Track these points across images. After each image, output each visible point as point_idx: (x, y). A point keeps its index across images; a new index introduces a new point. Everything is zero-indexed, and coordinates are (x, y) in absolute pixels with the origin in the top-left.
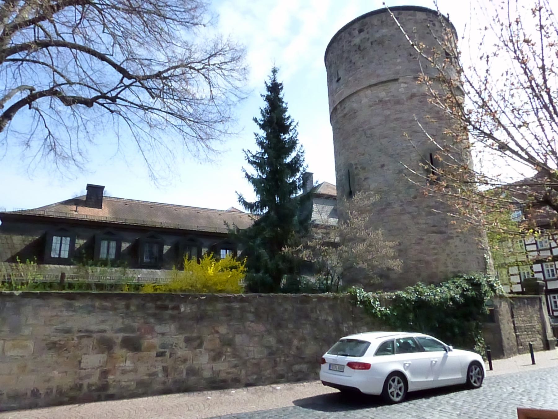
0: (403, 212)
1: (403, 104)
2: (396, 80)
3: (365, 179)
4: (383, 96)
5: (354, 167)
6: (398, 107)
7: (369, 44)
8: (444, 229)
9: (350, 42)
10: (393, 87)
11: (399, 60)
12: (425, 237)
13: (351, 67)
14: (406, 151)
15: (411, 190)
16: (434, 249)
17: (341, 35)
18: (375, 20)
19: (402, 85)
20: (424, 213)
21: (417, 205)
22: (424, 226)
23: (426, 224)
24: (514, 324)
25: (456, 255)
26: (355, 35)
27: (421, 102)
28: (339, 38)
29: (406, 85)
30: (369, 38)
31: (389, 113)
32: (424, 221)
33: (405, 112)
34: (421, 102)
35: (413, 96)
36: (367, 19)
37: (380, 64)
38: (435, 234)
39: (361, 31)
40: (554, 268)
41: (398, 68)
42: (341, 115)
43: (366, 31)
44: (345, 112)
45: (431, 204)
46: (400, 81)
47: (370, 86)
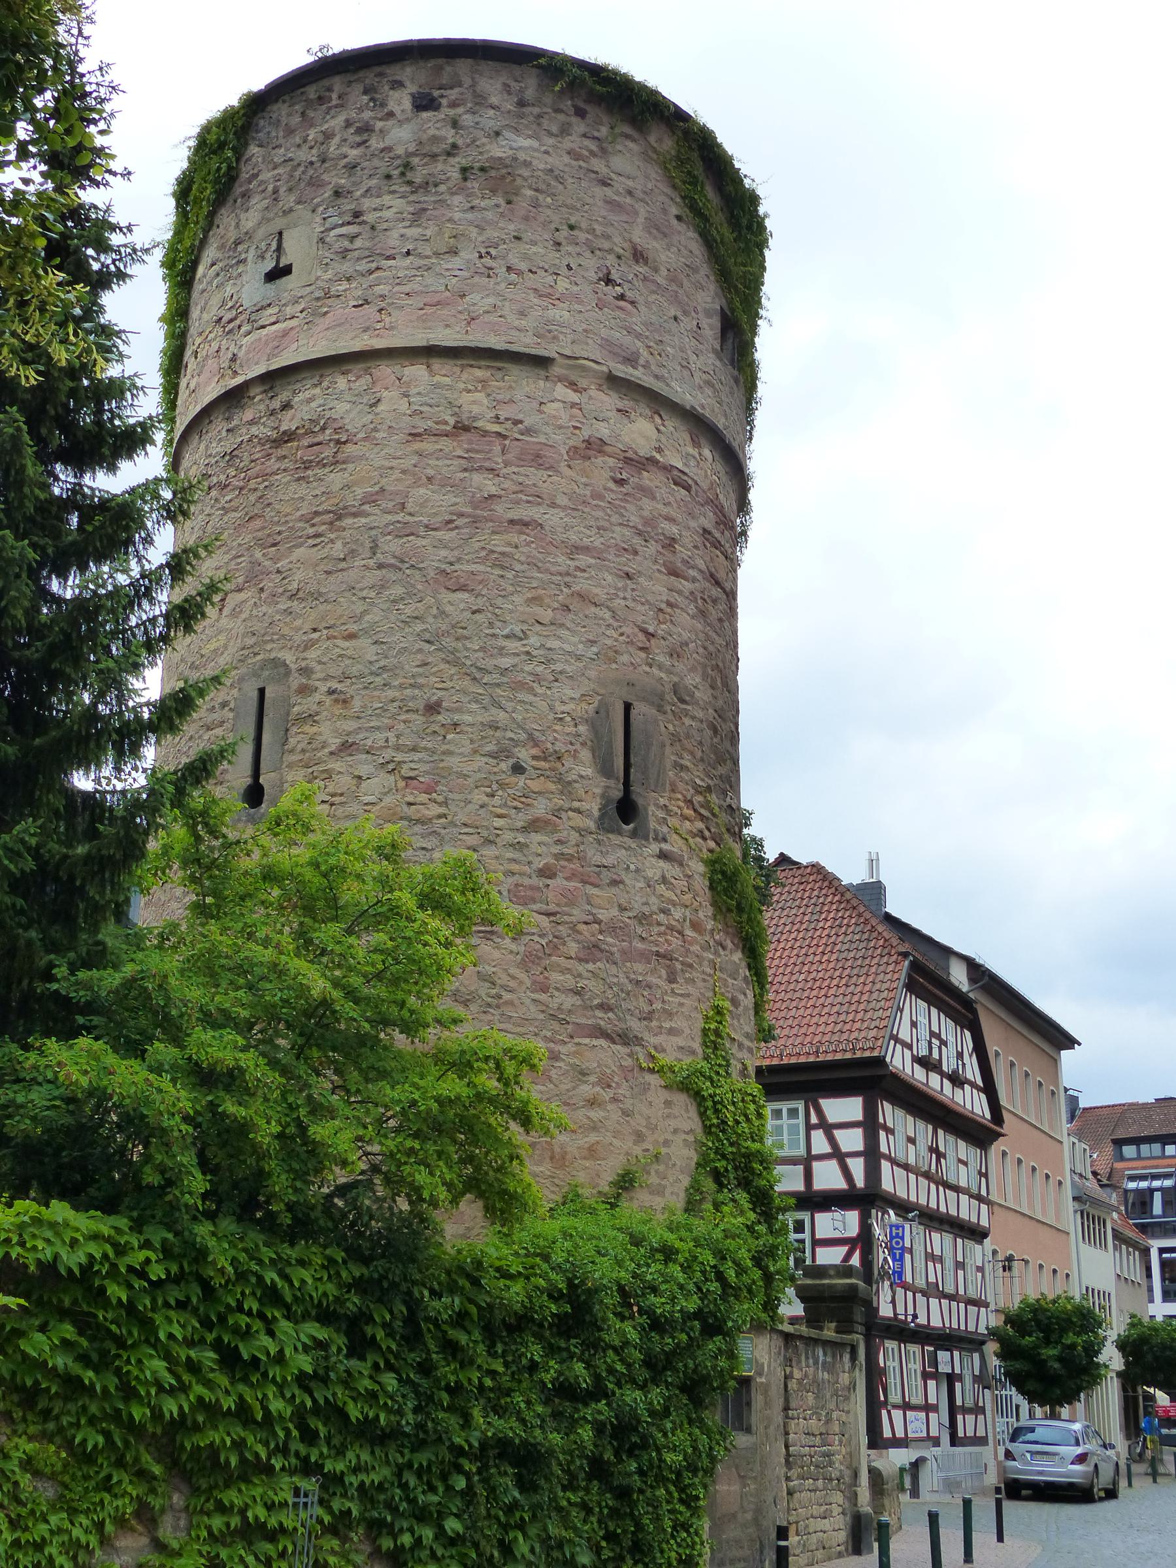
2: (541, 362)
3: (347, 747)
4: (476, 409)
5: (296, 681)
6: (534, 476)
7: (456, 175)
8: (635, 1025)
9: (366, 129)
10: (523, 385)
12: (563, 1049)
13: (352, 238)
14: (540, 669)
15: (536, 838)
16: (592, 1103)
17: (326, 82)
18: (493, 84)
19: (561, 391)
20: (573, 948)
21: (552, 908)
22: (569, 1001)
23: (578, 992)
24: (787, 1447)
25: (666, 1143)
26: (392, 106)
27: (621, 482)
28: (312, 92)
29: (573, 397)
30: (454, 146)
31: (494, 490)
32: (569, 981)
33: (553, 505)
34: (621, 482)
35: (594, 447)
36: (462, 67)
37: (489, 272)
38: (602, 1042)
39: (424, 103)
40: (806, 1236)
41: (553, 313)
43: (446, 112)
44: (288, 422)
45: (603, 915)
46: (556, 370)
47: (429, 352)
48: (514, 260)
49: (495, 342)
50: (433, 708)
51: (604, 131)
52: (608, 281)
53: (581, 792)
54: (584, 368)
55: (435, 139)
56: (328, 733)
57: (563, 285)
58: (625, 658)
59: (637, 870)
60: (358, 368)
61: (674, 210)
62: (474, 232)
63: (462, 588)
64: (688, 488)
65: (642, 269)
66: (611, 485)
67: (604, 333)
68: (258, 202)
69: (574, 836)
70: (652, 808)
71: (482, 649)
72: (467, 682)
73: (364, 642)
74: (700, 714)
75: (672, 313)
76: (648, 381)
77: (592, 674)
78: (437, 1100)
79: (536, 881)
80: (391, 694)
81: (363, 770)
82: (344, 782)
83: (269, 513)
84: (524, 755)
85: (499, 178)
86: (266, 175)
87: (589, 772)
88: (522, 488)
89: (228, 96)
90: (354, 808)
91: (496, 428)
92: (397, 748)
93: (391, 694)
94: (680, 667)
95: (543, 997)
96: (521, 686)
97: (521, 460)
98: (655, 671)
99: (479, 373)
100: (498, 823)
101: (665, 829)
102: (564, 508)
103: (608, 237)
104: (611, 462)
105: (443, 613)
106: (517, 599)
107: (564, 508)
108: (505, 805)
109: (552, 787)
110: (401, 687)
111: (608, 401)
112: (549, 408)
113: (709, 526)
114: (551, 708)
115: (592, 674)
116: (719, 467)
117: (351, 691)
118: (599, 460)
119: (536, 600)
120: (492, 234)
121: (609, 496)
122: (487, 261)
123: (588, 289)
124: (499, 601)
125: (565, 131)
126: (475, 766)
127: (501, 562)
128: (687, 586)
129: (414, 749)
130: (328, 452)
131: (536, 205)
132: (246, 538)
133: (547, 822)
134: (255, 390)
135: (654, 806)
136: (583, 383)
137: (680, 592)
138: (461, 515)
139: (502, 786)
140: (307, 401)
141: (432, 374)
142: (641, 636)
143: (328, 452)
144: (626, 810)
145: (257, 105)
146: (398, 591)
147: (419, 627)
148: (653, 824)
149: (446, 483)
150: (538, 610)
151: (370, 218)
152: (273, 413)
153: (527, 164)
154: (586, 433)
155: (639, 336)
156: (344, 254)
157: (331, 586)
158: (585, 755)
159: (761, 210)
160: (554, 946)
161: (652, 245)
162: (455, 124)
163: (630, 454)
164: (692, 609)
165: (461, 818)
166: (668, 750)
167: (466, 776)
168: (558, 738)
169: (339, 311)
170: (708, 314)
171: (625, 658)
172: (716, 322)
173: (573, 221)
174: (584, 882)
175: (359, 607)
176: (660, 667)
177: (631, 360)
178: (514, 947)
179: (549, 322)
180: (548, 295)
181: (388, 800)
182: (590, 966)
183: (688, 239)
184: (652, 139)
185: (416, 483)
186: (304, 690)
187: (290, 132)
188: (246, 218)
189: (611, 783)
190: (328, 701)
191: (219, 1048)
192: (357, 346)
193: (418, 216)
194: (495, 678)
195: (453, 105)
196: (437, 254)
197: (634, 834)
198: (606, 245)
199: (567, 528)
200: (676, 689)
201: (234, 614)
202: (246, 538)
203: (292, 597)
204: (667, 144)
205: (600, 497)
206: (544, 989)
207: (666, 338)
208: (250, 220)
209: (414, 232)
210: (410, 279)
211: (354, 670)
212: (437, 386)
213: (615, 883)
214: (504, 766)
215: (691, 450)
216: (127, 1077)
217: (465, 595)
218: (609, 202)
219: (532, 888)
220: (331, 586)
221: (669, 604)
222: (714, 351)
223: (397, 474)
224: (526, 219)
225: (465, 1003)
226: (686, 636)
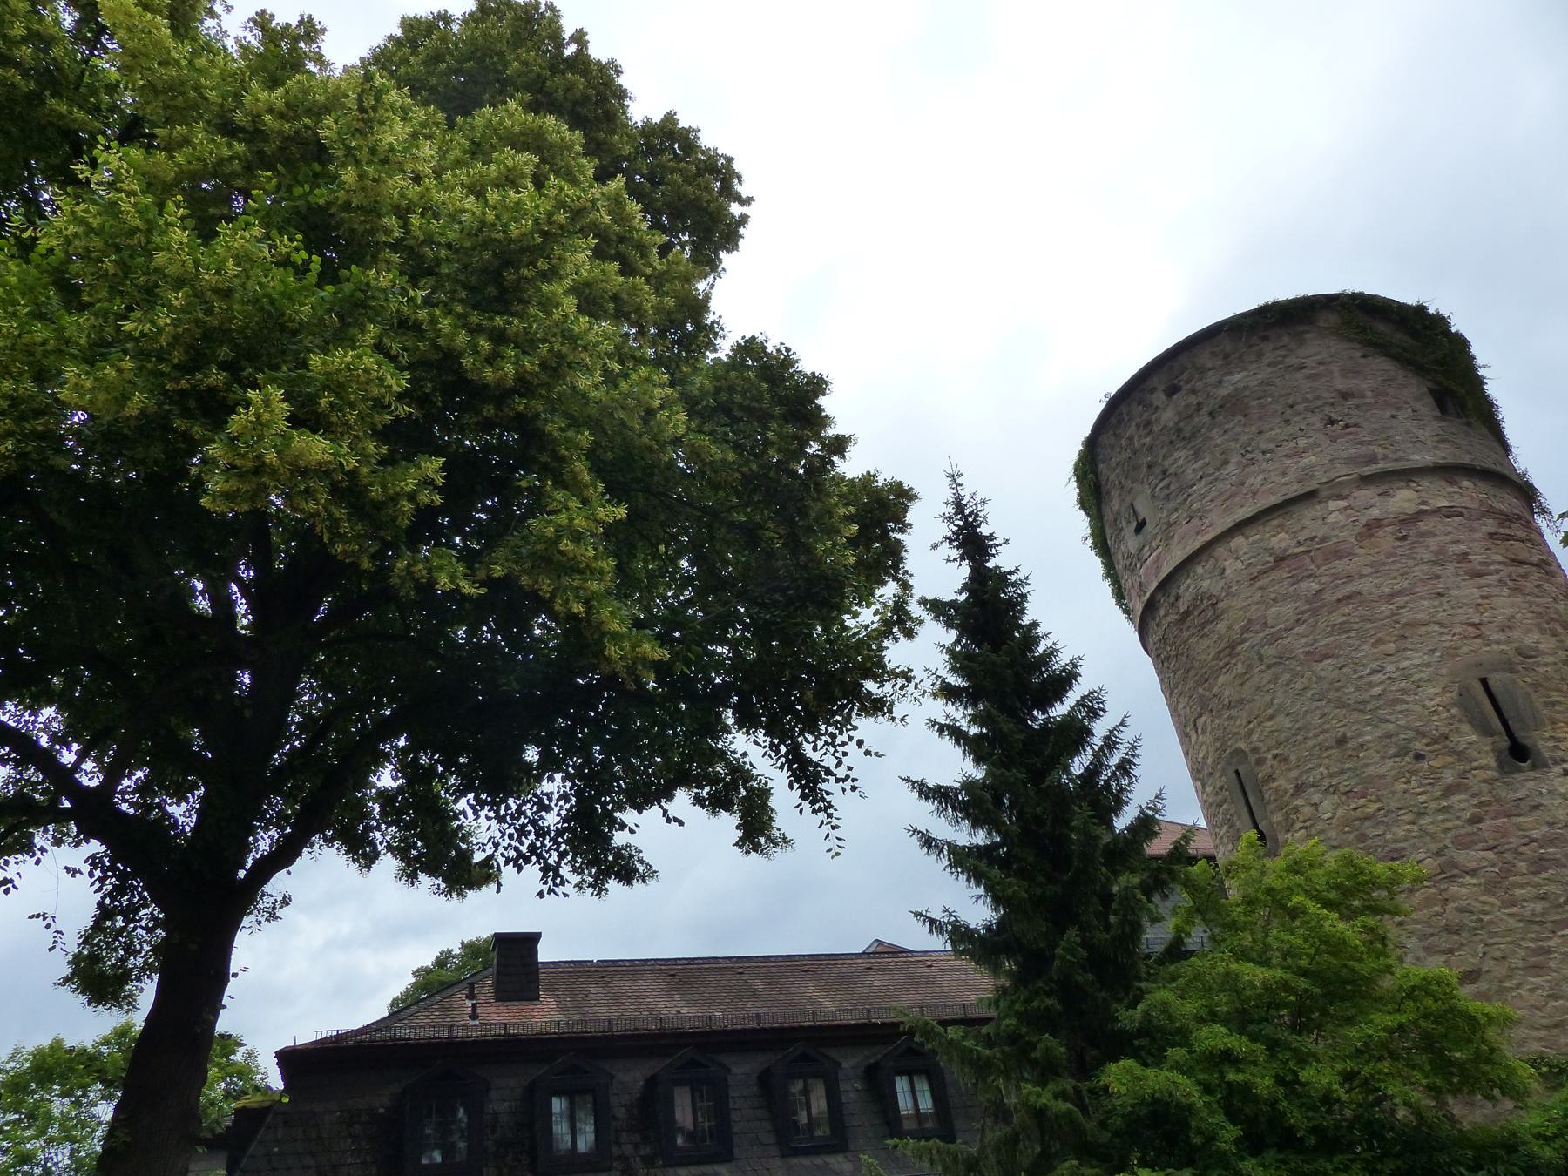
0: (1450, 872)
1: (1351, 554)
2: (1310, 496)
3: (1299, 789)
4: (1283, 545)
5: (1252, 758)
6: (1340, 565)
7: (1206, 419)
9: (1148, 423)
11: (1302, 443)
12: (1551, 943)
13: (1168, 486)
14: (1403, 685)
15: (1456, 798)
18: (1204, 358)
19: (1333, 505)
20: (1523, 866)
21: (1491, 843)
22: (1539, 907)
23: (1543, 897)
26: (1156, 403)
27: (1404, 538)
28: (1113, 421)
29: (1344, 503)
30: (1199, 404)
31: (1317, 587)
33: (1362, 576)
34: (1404, 538)
35: (1373, 526)
36: (1183, 359)
37: (1253, 462)
39: (1172, 391)
41: (1306, 461)
42: (1173, 617)
45: (1535, 834)
46: (1324, 494)
47: (1239, 527)
48: (1263, 446)
49: (1274, 500)
50: (1342, 741)
51: (1286, 339)
52: (1332, 422)
53: (1475, 754)
54: (1340, 483)
55: (1187, 406)
56: (1284, 783)
57: (1302, 443)
58: (1465, 650)
59: (1550, 792)
60: (1204, 557)
61: (1359, 354)
62: (1232, 445)
63: (1326, 657)
64: (1461, 515)
65: (1351, 402)
66: (1398, 543)
67: (1344, 455)
68: (1115, 493)
69: (1485, 787)
70: (1541, 744)
71: (1357, 689)
72: (1356, 716)
73: (1280, 718)
74: (1551, 659)
75: (1388, 414)
76: (1390, 466)
77: (1444, 671)
78: (1384, 1029)
79: (1469, 829)
80: (1310, 743)
81: (1316, 798)
82: (1307, 810)
83: (1196, 664)
84: (1418, 746)
85: (1234, 405)
86: (1112, 477)
87: (1474, 738)
88: (1336, 576)
89: (1074, 449)
90: (1320, 826)
91: (1301, 549)
92: (1331, 776)
93: (1310, 743)
94: (1515, 634)
95: (1515, 910)
96: (1395, 702)
97: (1327, 560)
98: (1495, 647)
99: (1274, 523)
100: (1422, 798)
101: (1560, 753)
102: (1370, 575)
103: (1318, 398)
104: (1390, 529)
105: (1320, 678)
106: (1365, 647)
107: (1370, 575)
108: (1421, 785)
109: (1450, 759)
110: (1316, 736)
111: (1368, 494)
112: (1332, 518)
113: (1491, 529)
114: (1424, 707)
115: (1444, 671)
116: (1482, 486)
117: (1286, 751)
118: (1381, 533)
119: (1380, 641)
120: (1244, 438)
121: (1399, 552)
122: (1249, 456)
123: (1320, 435)
124: (1354, 654)
125: (1260, 355)
126: (1388, 767)
127: (1343, 628)
128: (1492, 579)
129: (1342, 772)
130: (1210, 613)
131: (1262, 407)
132: (1190, 684)
133: (1459, 785)
134: (1159, 596)
135: (1540, 740)
136: (1346, 492)
137: (1488, 586)
138: (1304, 612)
139: (1413, 773)
140: (1187, 590)
141: (1247, 538)
142: (1471, 629)
143: (1210, 613)
144: (1518, 753)
145: (1092, 444)
146: (1287, 676)
147: (1309, 694)
148: (1547, 754)
149: (1285, 598)
150: (1382, 647)
151: (1172, 470)
152: (1172, 605)
153: (1246, 388)
154: (1364, 521)
155: (1370, 443)
156: (1167, 497)
157: (1246, 691)
158: (1465, 727)
159: (1432, 311)
160: (1508, 869)
161: (1352, 383)
162: (1194, 392)
163: (1402, 517)
164: (1506, 591)
165: (1394, 805)
166: (1534, 696)
167: (1384, 777)
168: (1439, 724)
169: (1180, 531)
170: (1418, 399)
171: (1465, 650)
172: (1430, 400)
173: (1290, 401)
174: (1509, 816)
175: (1268, 698)
176: (1498, 643)
177: (1373, 459)
178: (1474, 881)
179: (1304, 468)
180: (1297, 454)
181: (1340, 812)
182: (1544, 875)
183: (1381, 366)
184: (1321, 323)
185: (1267, 608)
186: (1260, 762)
187: (1113, 447)
188: (1115, 504)
189: (1497, 738)
190: (1275, 763)
191: (1215, 1037)
192: (1197, 545)
193: (1197, 455)
194: (1374, 704)
195: (1188, 382)
196: (1218, 469)
197: (1534, 767)
198: (1319, 403)
199: (1378, 586)
200: (1519, 652)
201: (1204, 732)
202: (1190, 684)
203: (1229, 707)
204: (1333, 319)
205: (1394, 555)
206: (1514, 904)
207: (1392, 432)
208: (1115, 504)
209: (1200, 463)
210: (1209, 492)
211: (1283, 736)
212: (1254, 542)
213: (1536, 807)
214: (1408, 759)
215: (1450, 489)
216: (1157, 1079)
217: (1329, 661)
218: (1310, 377)
219: (1469, 834)
220: (1246, 691)
221: (1483, 597)
222: (1436, 418)
223: (1254, 607)
224: (1260, 418)
225: (1457, 933)
226: (1508, 612)
